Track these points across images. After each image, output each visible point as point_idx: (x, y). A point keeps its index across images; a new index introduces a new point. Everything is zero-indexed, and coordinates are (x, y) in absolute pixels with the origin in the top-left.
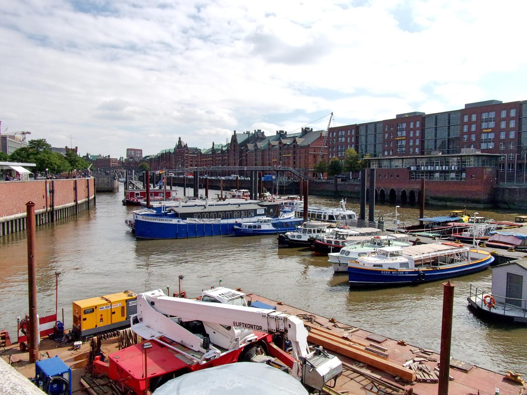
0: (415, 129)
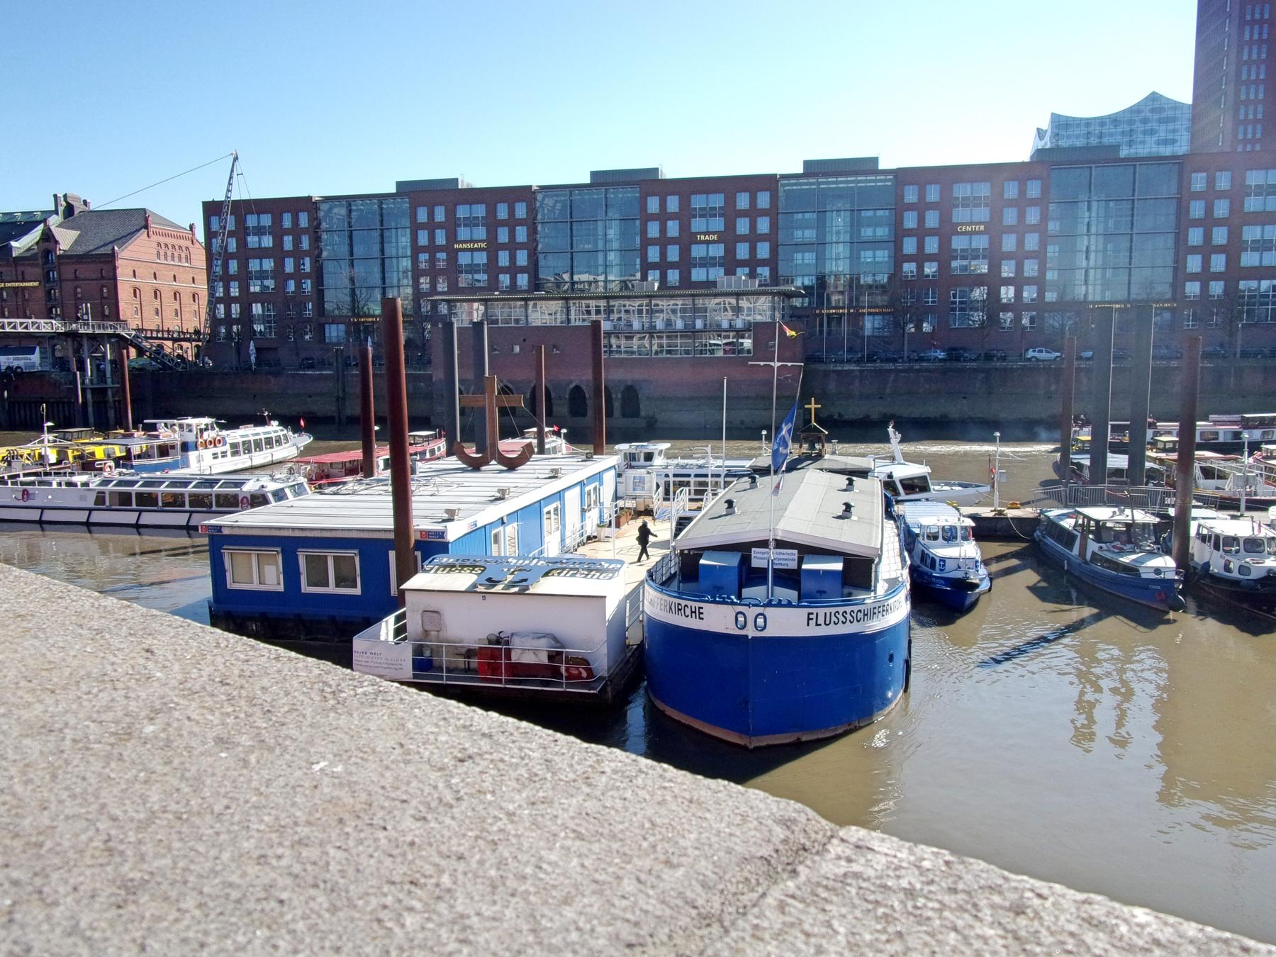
0: (512, 223)
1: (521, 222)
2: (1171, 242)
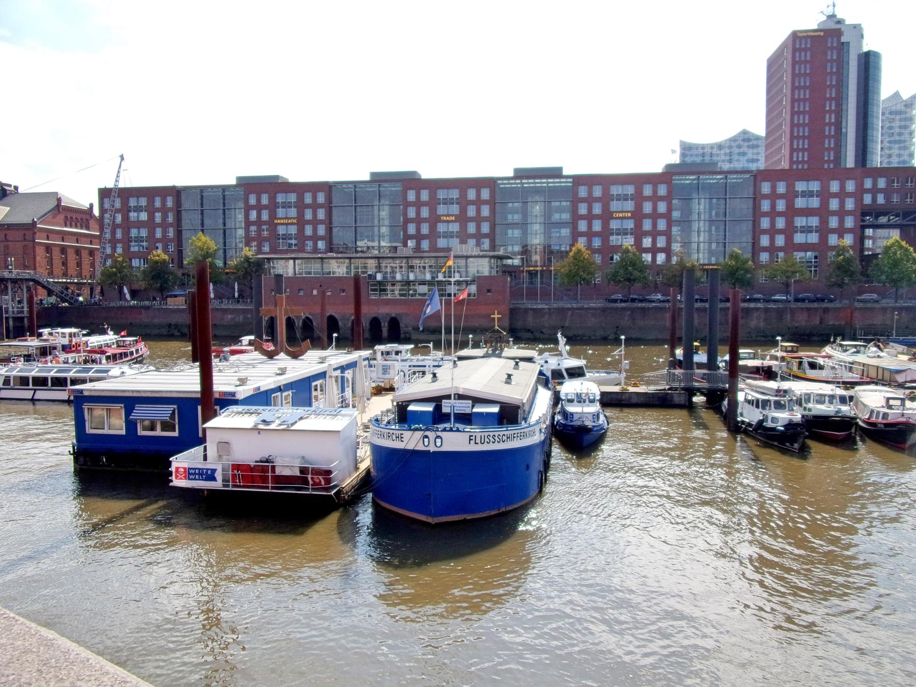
0: (315, 206)
1: (321, 206)
2: (750, 227)
